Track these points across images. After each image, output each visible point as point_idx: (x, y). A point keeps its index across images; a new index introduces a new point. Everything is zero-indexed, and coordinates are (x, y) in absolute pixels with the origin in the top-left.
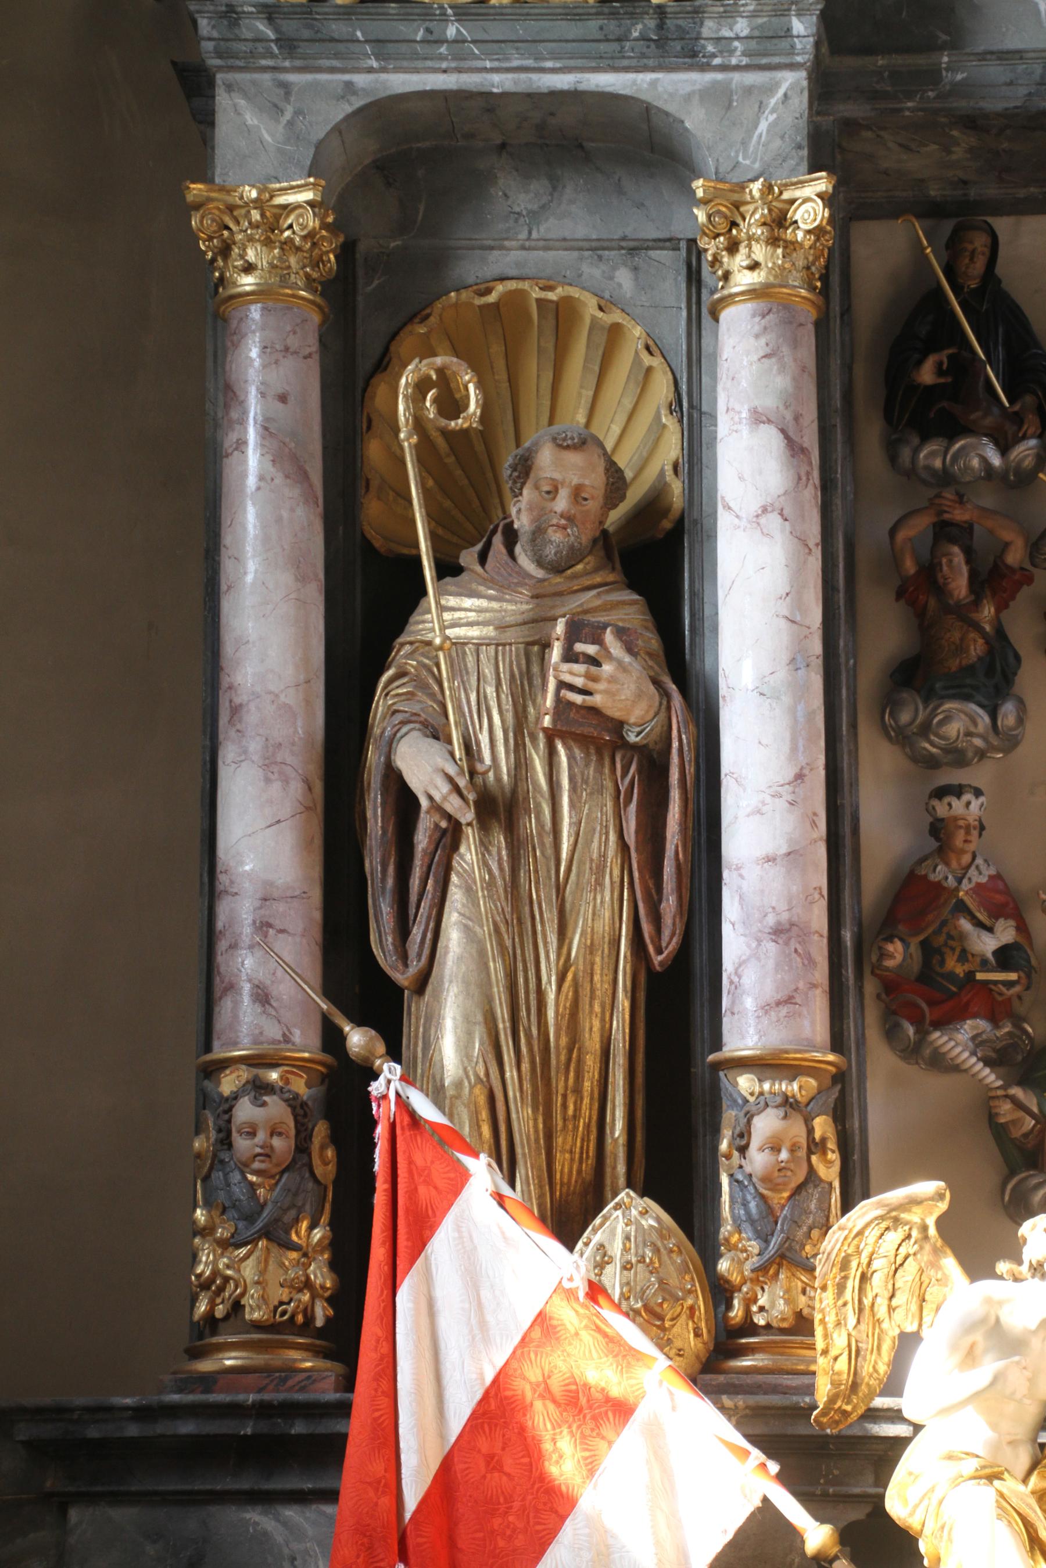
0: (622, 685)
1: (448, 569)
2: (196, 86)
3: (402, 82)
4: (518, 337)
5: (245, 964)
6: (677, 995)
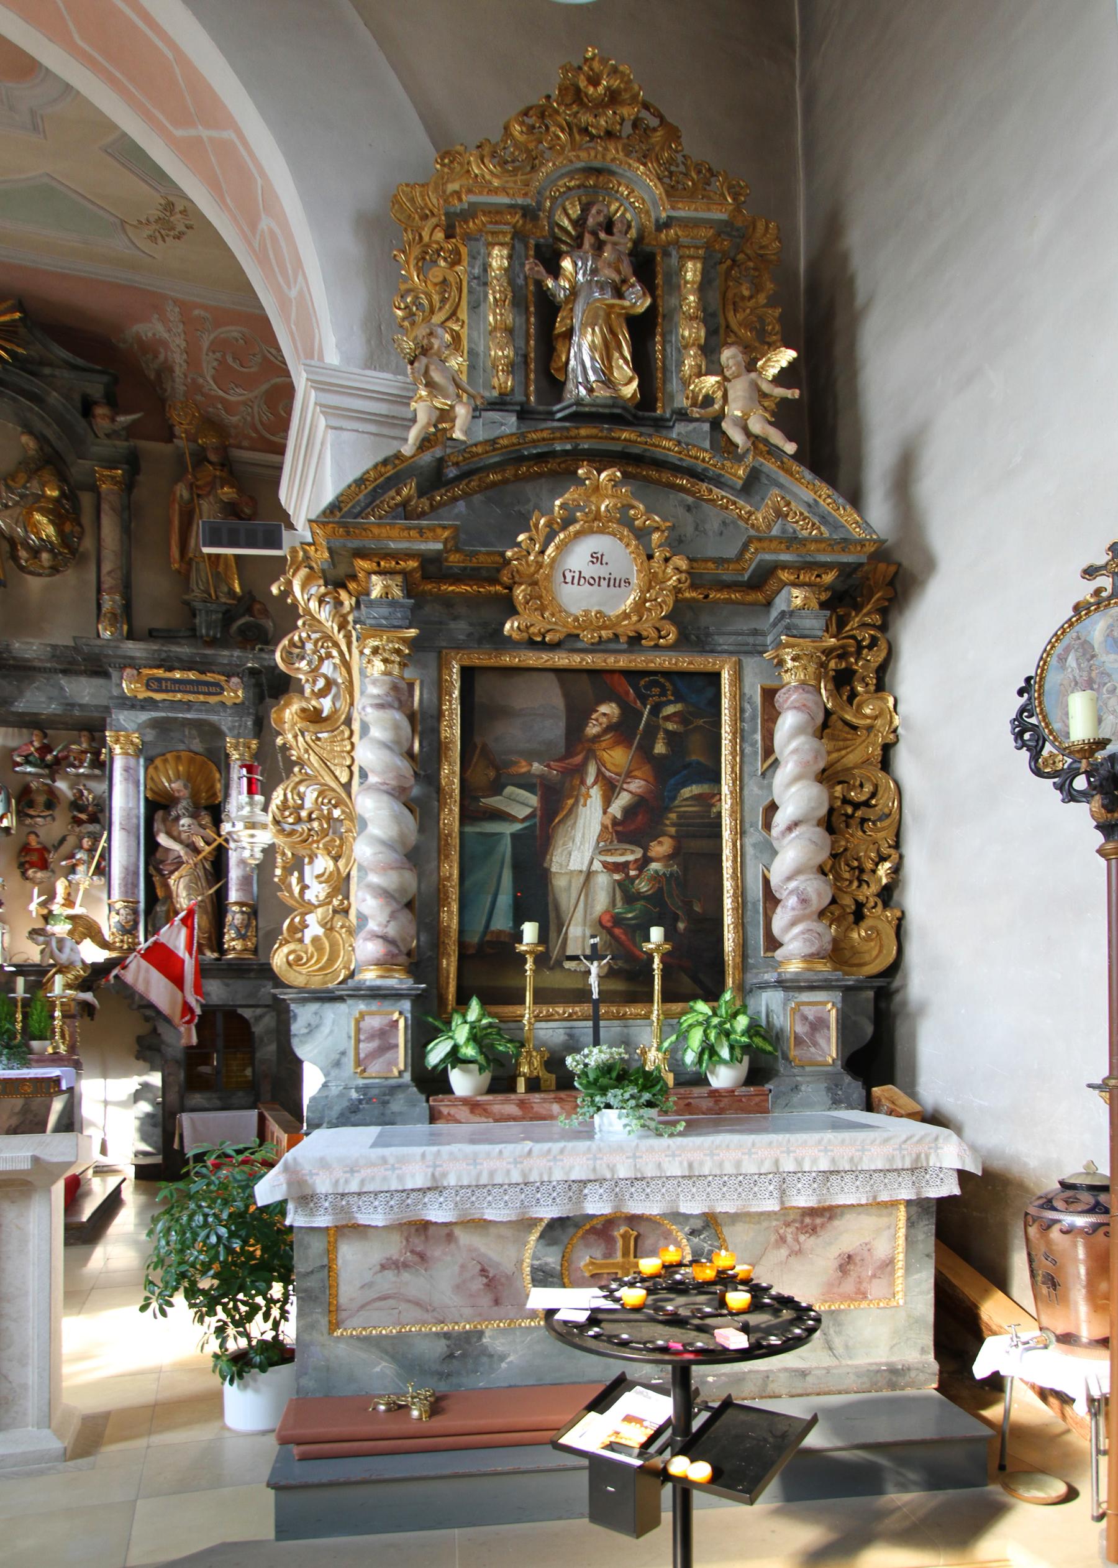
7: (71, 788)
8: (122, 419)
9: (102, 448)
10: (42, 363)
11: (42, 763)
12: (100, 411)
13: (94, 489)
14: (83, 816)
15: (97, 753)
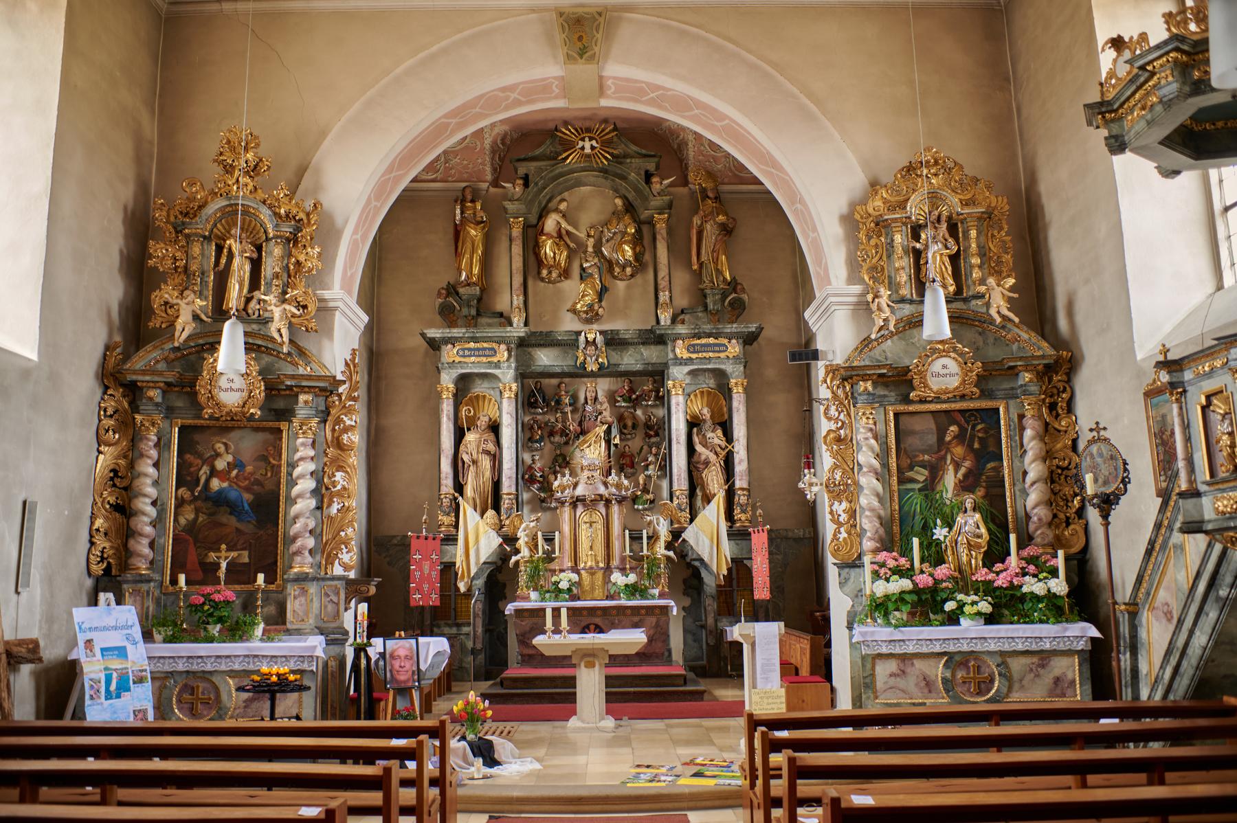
0: (491, 447)
1: (469, 429)
2: (439, 372)
5: (443, 482)
6: (497, 485)
7: (644, 413)
8: (666, 182)
9: (656, 202)
11: (629, 400)
12: (655, 179)
13: (650, 223)
15: (658, 391)
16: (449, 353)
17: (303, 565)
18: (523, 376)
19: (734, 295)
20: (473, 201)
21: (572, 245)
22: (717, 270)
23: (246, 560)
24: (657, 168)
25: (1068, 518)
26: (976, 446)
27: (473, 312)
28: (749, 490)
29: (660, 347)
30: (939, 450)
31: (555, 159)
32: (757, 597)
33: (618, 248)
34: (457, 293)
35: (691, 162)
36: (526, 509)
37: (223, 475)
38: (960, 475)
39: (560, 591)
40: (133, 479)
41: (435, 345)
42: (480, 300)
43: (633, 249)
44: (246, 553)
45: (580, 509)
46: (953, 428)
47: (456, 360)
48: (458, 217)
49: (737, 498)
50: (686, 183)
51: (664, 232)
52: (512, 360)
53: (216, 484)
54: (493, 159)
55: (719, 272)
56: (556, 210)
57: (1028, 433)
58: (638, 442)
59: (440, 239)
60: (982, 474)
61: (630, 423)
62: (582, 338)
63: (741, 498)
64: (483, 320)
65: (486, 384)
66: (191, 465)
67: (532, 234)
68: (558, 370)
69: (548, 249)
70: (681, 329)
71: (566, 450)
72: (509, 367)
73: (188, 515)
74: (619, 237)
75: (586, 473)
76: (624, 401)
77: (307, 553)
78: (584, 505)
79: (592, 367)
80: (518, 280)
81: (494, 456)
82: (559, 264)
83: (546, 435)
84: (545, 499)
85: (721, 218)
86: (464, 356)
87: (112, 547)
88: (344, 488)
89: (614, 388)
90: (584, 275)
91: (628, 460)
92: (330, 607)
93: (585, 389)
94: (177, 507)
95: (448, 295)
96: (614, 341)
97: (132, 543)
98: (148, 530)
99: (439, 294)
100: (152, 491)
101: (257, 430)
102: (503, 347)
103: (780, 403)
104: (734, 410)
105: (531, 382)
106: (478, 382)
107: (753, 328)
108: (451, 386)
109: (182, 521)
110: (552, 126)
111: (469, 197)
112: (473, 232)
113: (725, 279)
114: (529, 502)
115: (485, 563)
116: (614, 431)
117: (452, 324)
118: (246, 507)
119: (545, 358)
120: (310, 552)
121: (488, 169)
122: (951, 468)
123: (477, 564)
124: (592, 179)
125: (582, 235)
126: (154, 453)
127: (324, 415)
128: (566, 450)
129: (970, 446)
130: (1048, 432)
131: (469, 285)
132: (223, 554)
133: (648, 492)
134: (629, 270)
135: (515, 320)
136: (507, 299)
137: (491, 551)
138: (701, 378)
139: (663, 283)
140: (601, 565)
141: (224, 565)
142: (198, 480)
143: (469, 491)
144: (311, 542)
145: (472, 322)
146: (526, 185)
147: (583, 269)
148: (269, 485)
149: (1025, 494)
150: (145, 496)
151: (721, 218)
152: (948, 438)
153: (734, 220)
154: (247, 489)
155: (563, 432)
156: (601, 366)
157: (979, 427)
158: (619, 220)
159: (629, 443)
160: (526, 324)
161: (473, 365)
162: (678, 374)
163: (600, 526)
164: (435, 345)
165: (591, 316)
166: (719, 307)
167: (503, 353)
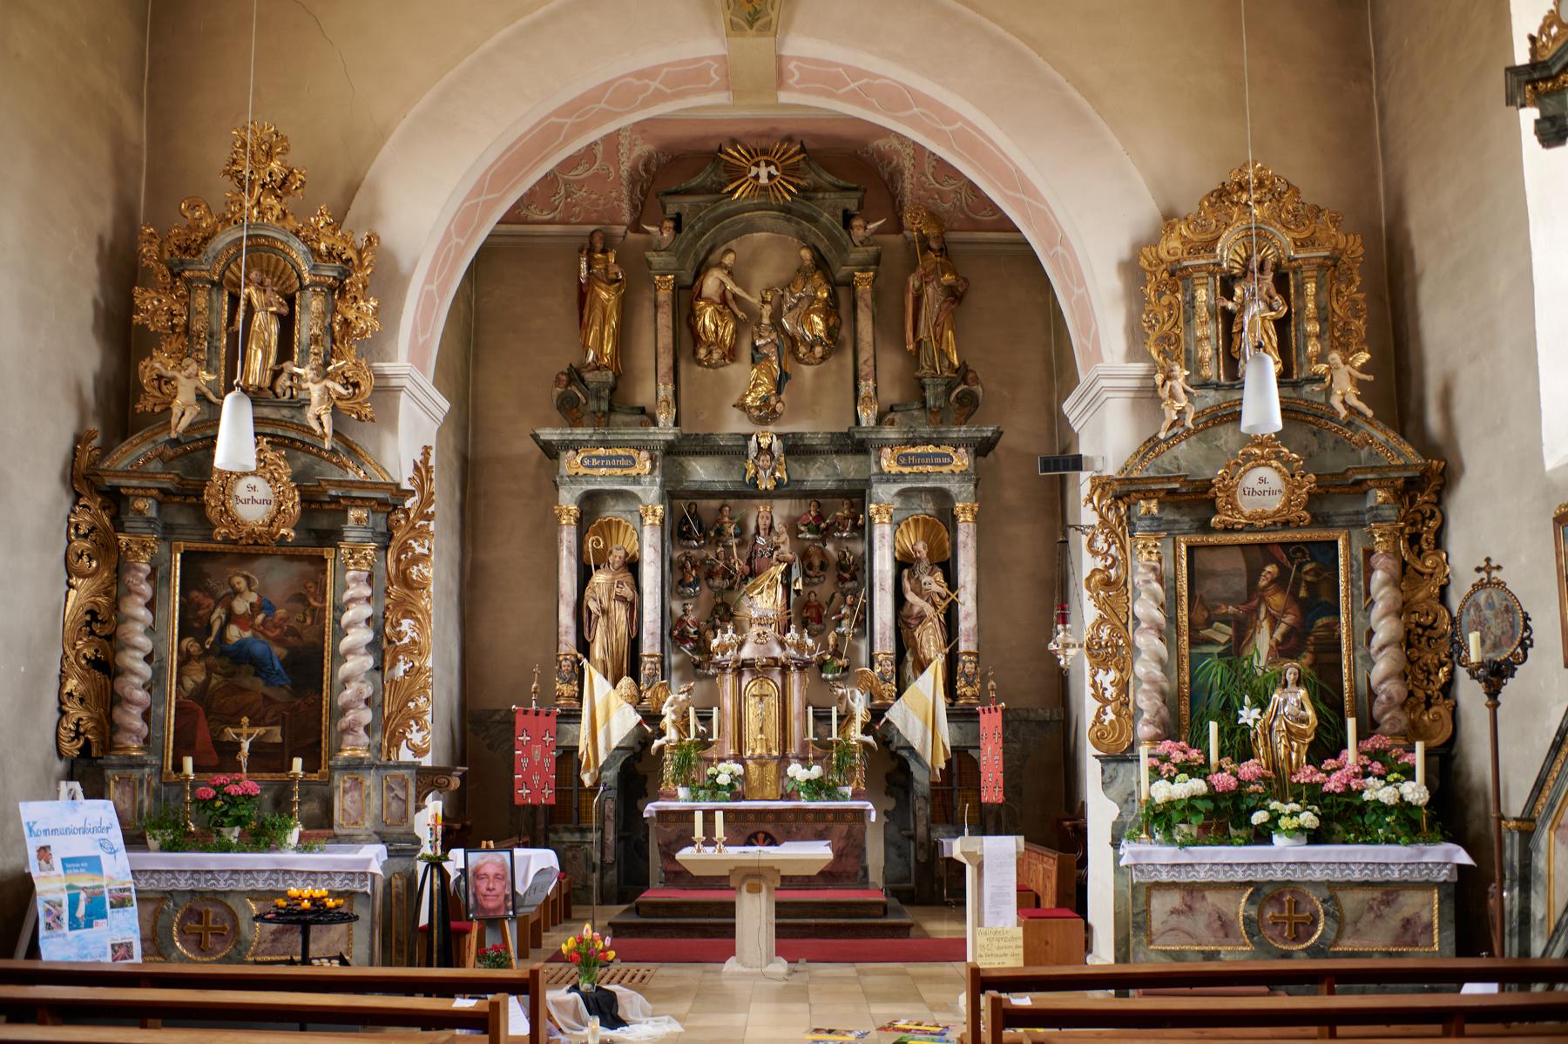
0: (627, 591)
1: (597, 568)
3: (591, 487)
4: (608, 528)
5: (562, 638)
6: (635, 643)
8: (872, 226)
9: (859, 254)
10: (816, 189)
11: (816, 530)
12: (857, 223)
14: (847, 576)
15: (856, 519)
16: (571, 463)
17: (356, 746)
18: (670, 495)
19: (963, 387)
20: (604, 251)
21: (740, 314)
22: (941, 351)
23: (278, 739)
24: (860, 206)
25: (1429, 697)
26: (1303, 593)
27: (604, 406)
28: (977, 655)
29: (860, 458)
30: (1250, 599)
31: (719, 192)
32: (985, 798)
33: (805, 319)
34: (582, 380)
35: (908, 198)
36: (675, 677)
37: (244, 621)
38: (1278, 635)
39: (719, 787)
40: (118, 624)
41: (551, 451)
42: (613, 390)
43: (825, 321)
44: (277, 730)
45: (746, 678)
46: (1271, 569)
47: (581, 470)
48: (584, 274)
49: (961, 665)
50: (899, 228)
51: (868, 297)
52: (657, 472)
53: (234, 633)
54: (632, 192)
55: (943, 354)
56: (720, 265)
57: (1378, 576)
58: (828, 588)
59: (560, 304)
60: (1309, 634)
61: (817, 562)
62: (753, 444)
63: (967, 666)
64: (618, 418)
65: (621, 506)
66: (199, 606)
67: (686, 298)
68: (720, 487)
69: (707, 320)
70: (890, 433)
71: (728, 597)
72: (652, 483)
73: (196, 675)
74: (805, 303)
75: (755, 629)
76: (810, 531)
77: (362, 731)
78: (753, 672)
79: (766, 484)
80: (666, 362)
81: (632, 604)
82: (723, 340)
83: (702, 576)
84: (700, 665)
85: (948, 278)
86: (590, 467)
87: (90, 719)
88: (413, 642)
89: (796, 513)
90: (757, 357)
91: (812, 613)
92: (395, 806)
93: (757, 514)
94: (180, 665)
95: (570, 382)
96: (796, 448)
97: (117, 712)
98: (140, 695)
99: (558, 381)
100: (144, 642)
101: (291, 558)
102: (644, 454)
103: (1023, 538)
104: (960, 545)
105: (683, 505)
106: (611, 502)
107: (988, 432)
108: (573, 508)
109: (189, 684)
110: (714, 145)
111: (599, 246)
112: (604, 295)
113: (951, 364)
114: (678, 668)
115: (617, 748)
116: (795, 573)
117: (575, 423)
118: (278, 666)
119: (702, 471)
120: (367, 728)
121: (626, 206)
122: (1265, 624)
123: (607, 749)
124: (770, 222)
125: (755, 300)
126: (146, 589)
127: (385, 540)
128: (728, 597)
129: (1294, 595)
130: (1405, 575)
131: (598, 368)
132: (245, 730)
133: (840, 656)
134: (818, 350)
135: (662, 418)
136: (652, 389)
137: (626, 732)
138: (916, 501)
139: (865, 369)
140: (775, 753)
141: (246, 745)
142: (209, 627)
143: (597, 651)
144: (366, 716)
145: (603, 419)
146: (678, 228)
147: (756, 349)
148: (309, 637)
149: (1371, 662)
150: (135, 648)
151: (948, 278)
152: (1263, 583)
153: (966, 280)
154: (279, 641)
155: (727, 574)
156: (779, 482)
157: (1308, 567)
158: (806, 279)
159: (816, 589)
160: (676, 423)
161: (603, 479)
162: (884, 493)
163: (773, 701)
164: (551, 451)
165: (766, 414)
166: (941, 403)
167: (644, 464)
